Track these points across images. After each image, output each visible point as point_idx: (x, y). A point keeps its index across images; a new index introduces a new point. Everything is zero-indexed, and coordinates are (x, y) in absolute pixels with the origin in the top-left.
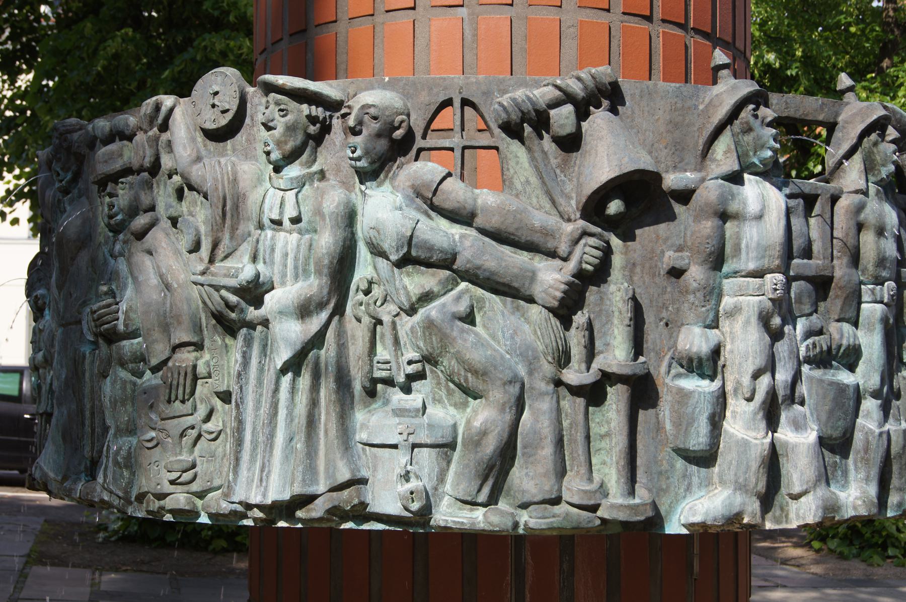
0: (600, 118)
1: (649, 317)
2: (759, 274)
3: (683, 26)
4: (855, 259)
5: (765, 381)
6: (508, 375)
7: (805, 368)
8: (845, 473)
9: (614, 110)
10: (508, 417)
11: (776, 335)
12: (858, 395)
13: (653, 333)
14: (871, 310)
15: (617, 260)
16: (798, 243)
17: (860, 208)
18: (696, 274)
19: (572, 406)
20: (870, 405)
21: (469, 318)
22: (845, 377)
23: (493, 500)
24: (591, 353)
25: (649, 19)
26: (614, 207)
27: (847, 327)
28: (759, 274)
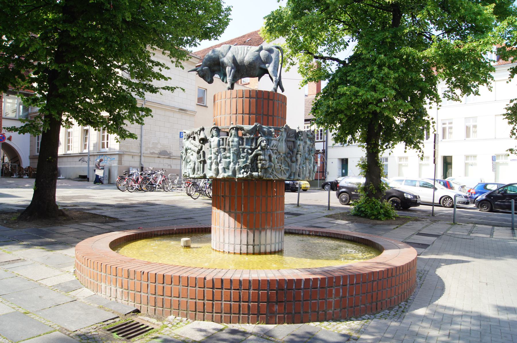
0: (202, 132)
1: (206, 154)
2: (214, 148)
3: (243, 114)
4: (229, 145)
5: (215, 160)
6: (193, 160)
7: (222, 159)
8: (229, 172)
9: (203, 131)
10: (194, 165)
11: (218, 155)
12: (230, 163)
13: (206, 156)
14: (231, 152)
15: (203, 148)
16: (221, 144)
17: (229, 139)
18: (209, 149)
19: (199, 164)
20: (232, 163)
21: (192, 155)
22: (228, 160)
23: (194, 174)
24: (200, 158)
25: (236, 114)
26: (201, 142)
27: (228, 154)
28: (214, 148)
